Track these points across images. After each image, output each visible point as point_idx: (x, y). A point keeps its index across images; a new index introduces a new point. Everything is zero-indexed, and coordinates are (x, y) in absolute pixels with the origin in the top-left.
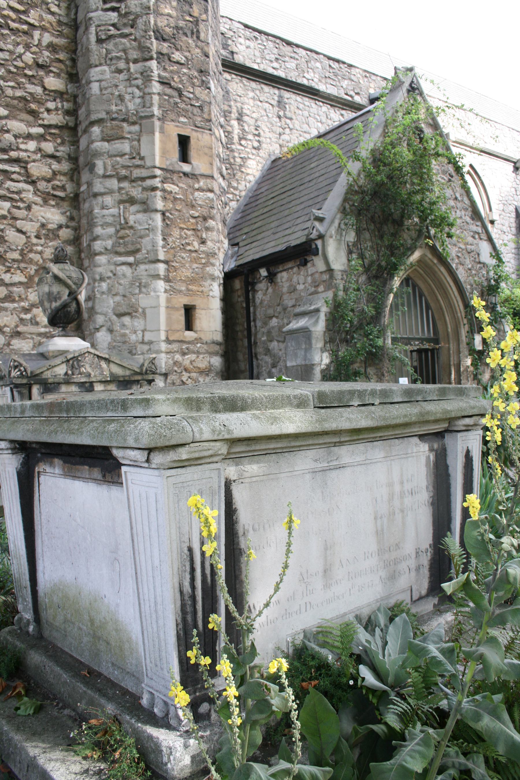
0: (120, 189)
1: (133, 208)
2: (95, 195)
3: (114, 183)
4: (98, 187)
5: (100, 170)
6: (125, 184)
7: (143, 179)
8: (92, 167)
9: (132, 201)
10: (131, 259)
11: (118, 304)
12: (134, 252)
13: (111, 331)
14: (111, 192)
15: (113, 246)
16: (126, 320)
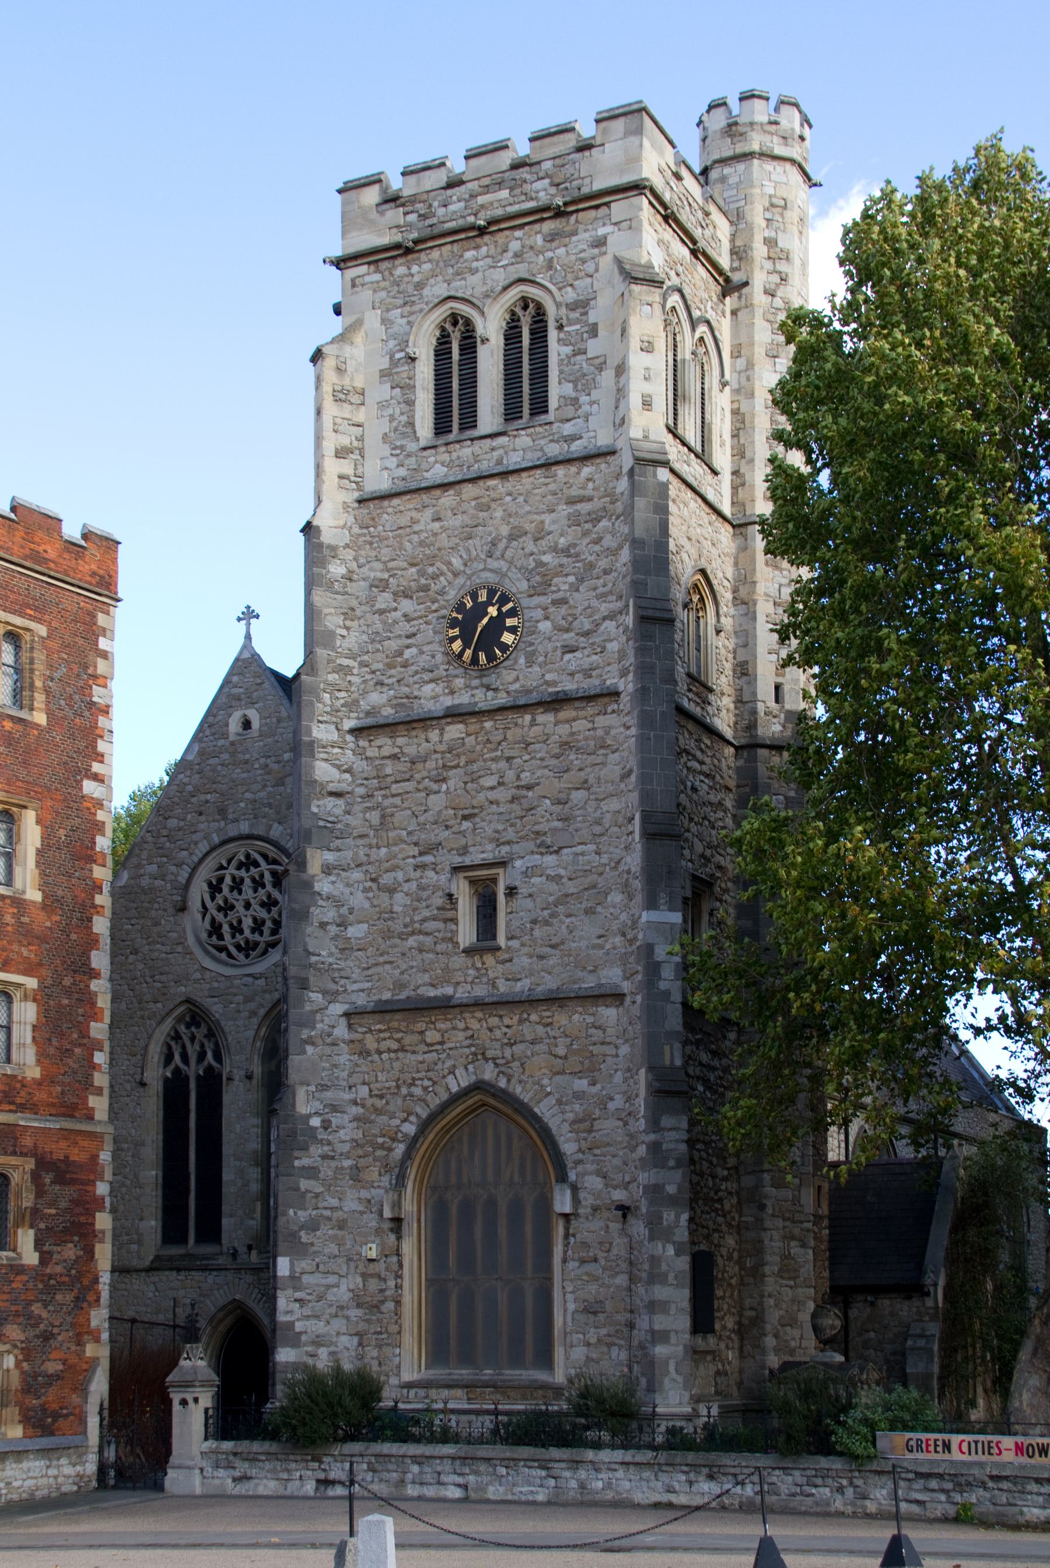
0: (784, 1227)
1: (793, 1243)
2: (765, 1230)
3: (780, 1223)
4: (768, 1224)
5: (769, 1210)
6: (788, 1223)
7: (802, 1222)
8: (762, 1207)
9: (793, 1238)
10: (792, 1283)
11: (782, 1317)
12: (794, 1279)
13: (776, 1336)
14: (777, 1229)
15: (780, 1271)
16: (788, 1328)
